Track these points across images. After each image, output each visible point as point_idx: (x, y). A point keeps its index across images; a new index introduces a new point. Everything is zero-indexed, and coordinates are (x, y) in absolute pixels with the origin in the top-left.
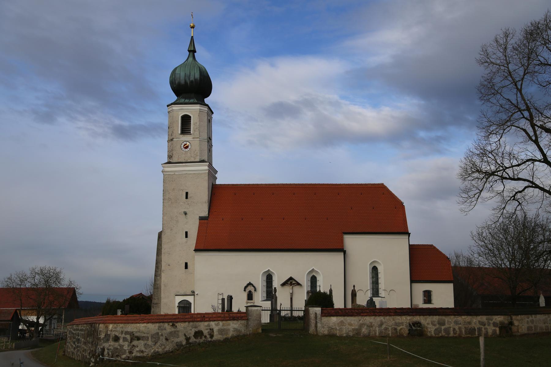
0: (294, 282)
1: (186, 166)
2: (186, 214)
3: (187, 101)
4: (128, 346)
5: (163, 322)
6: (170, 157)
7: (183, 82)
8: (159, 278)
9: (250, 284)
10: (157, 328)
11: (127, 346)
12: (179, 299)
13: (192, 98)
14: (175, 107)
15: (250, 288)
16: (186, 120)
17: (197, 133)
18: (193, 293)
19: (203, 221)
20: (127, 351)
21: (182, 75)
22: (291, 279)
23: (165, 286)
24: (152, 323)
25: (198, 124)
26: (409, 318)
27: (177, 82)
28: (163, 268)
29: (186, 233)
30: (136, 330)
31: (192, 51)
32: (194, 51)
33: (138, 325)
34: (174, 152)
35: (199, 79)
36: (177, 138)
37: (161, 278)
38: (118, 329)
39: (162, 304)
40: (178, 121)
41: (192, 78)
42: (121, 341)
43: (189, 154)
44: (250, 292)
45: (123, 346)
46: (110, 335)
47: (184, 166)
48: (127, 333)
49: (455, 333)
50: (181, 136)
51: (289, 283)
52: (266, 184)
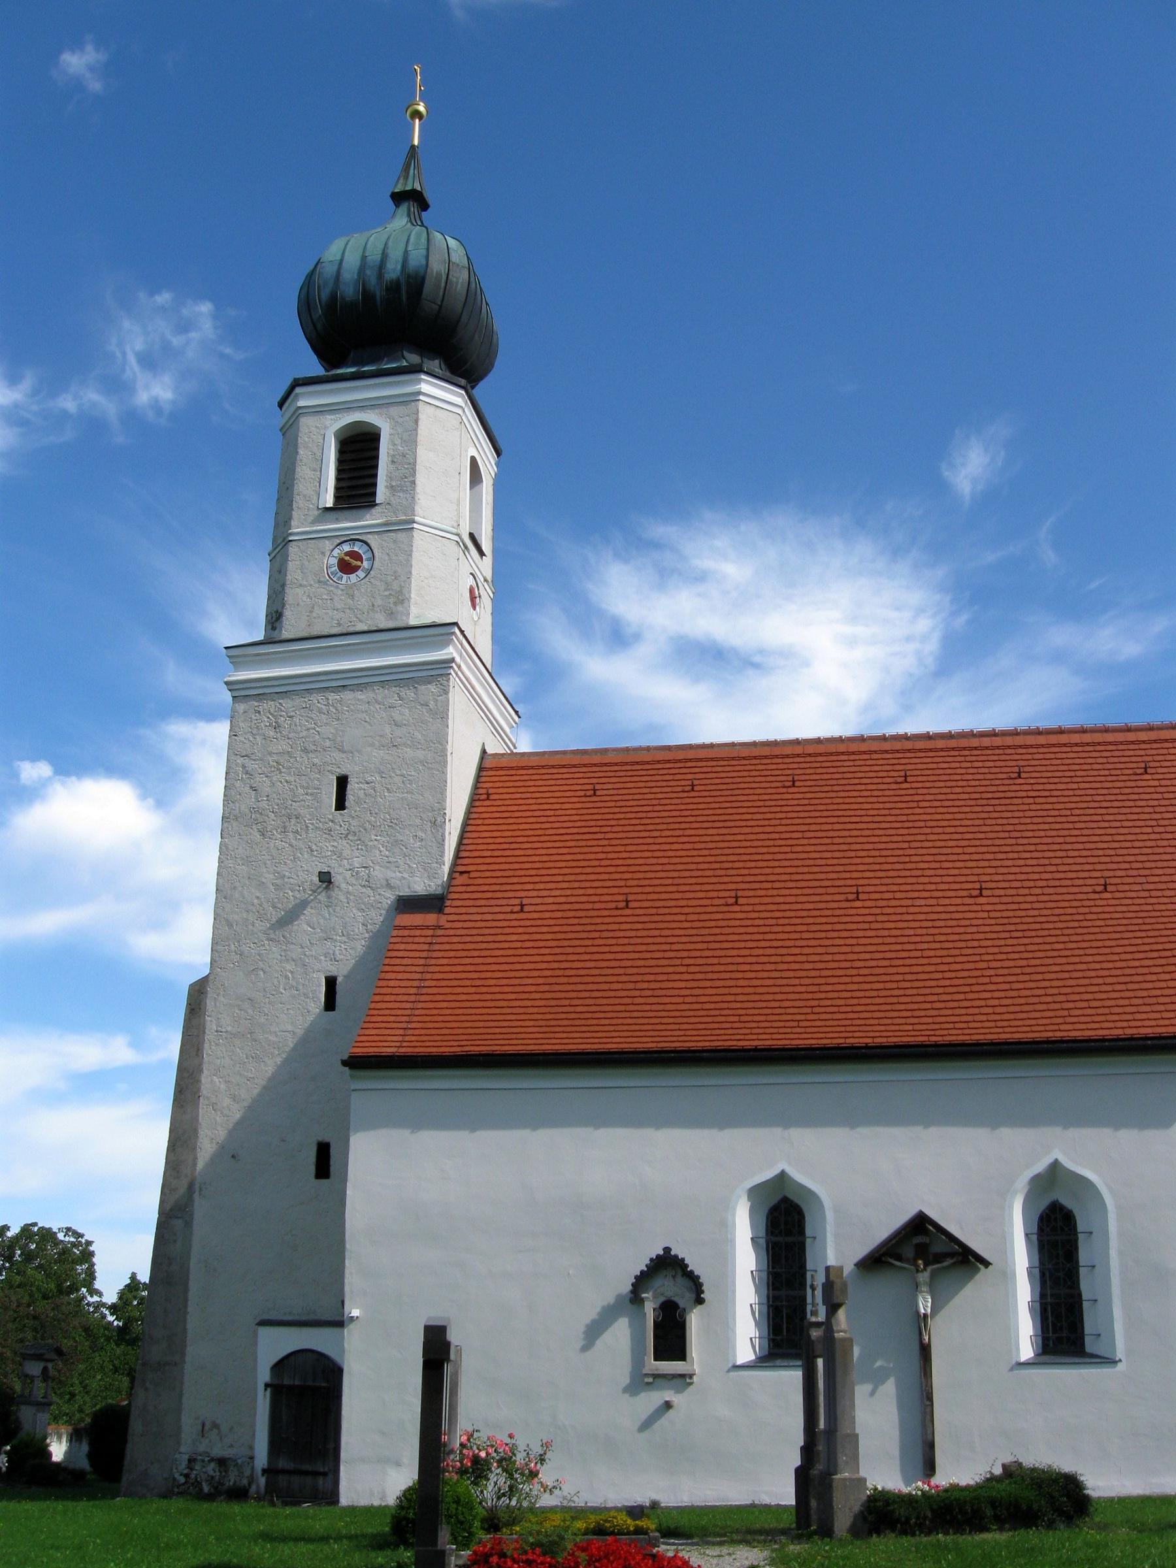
6: (275, 618)
7: (349, 291)
9: (667, 1264)
12: (276, 1344)
15: (668, 1287)
16: (359, 453)
22: (920, 1224)
37: (188, 1224)
39: (188, 1367)
43: (363, 601)
51: (909, 1252)
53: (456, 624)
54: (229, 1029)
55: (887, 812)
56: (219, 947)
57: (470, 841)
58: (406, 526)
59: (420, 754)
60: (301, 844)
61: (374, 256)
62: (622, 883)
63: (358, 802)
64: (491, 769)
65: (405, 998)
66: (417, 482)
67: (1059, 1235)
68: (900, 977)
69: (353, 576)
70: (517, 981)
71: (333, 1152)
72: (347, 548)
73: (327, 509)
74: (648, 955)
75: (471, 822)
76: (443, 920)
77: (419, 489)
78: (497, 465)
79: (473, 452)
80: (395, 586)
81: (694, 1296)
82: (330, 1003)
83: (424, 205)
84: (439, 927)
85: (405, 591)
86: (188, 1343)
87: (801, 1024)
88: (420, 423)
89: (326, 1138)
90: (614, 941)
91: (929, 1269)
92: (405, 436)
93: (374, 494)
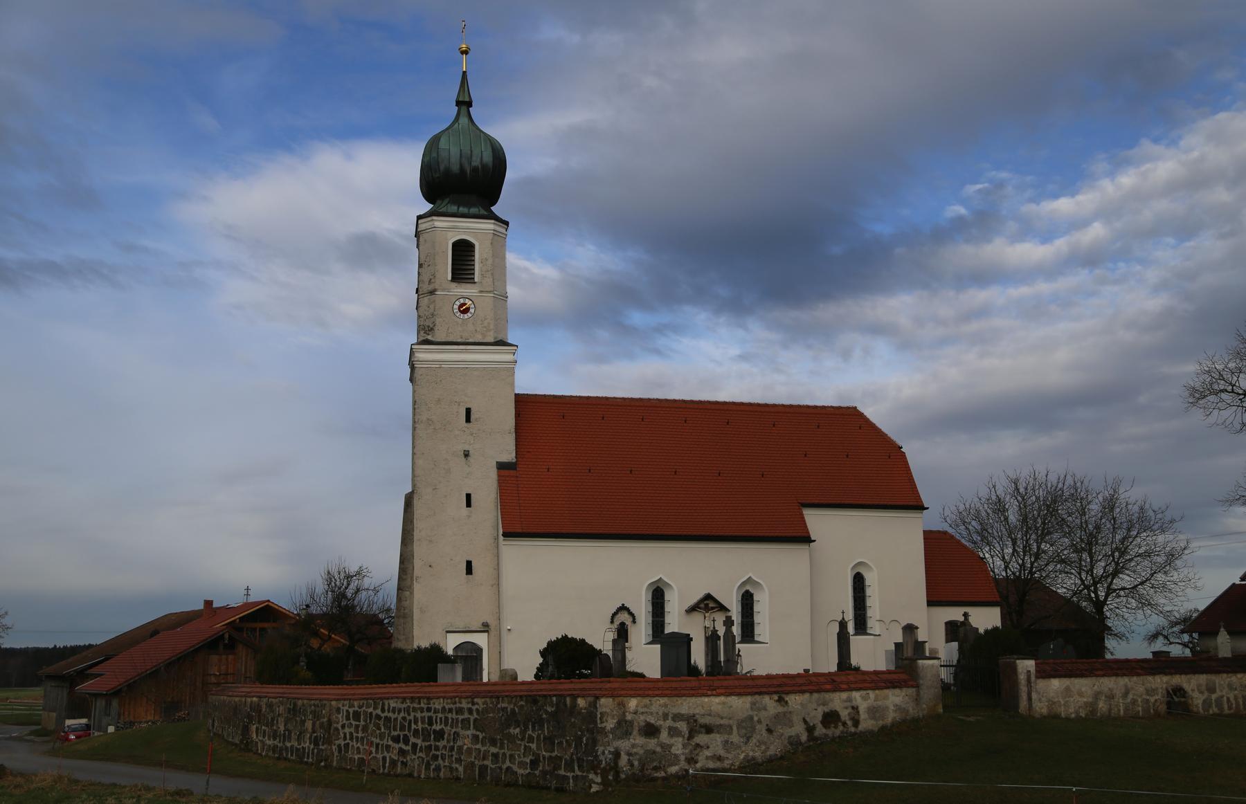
0: (711, 605)
1: (467, 351)
2: (466, 455)
3: (463, 210)
4: (684, 746)
5: (760, 693)
7: (455, 168)
8: (407, 593)
9: (623, 608)
10: (748, 705)
11: (680, 746)
13: (474, 205)
14: (440, 222)
15: (624, 617)
16: (463, 251)
17: (489, 280)
18: (485, 628)
19: (506, 472)
20: (682, 758)
21: (455, 152)
22: (708, 597)
23: (422, 611)
24: (739, 694)
25: (490, 262)
26: (1165, 679)
27: (442, 167)
28: (416, 572)
29: (468, 496)
30: (703, 712)
31: (464, 104)
32: (469, 104)
33: (706, 699)
34: (438, 321)
35: (491, 164)
36: (444, 290)
37: (412, 593)
38: (654, 709)
41: (476, 162)
42: (664, 735)
44: (623, 624)
45: (671, 746)
46: (631, 722)
47: (462, 351)
48: (677, 717)
49: (1230, 708)
50: (454, 285)
52: (624, 399)
67: (747, 601)
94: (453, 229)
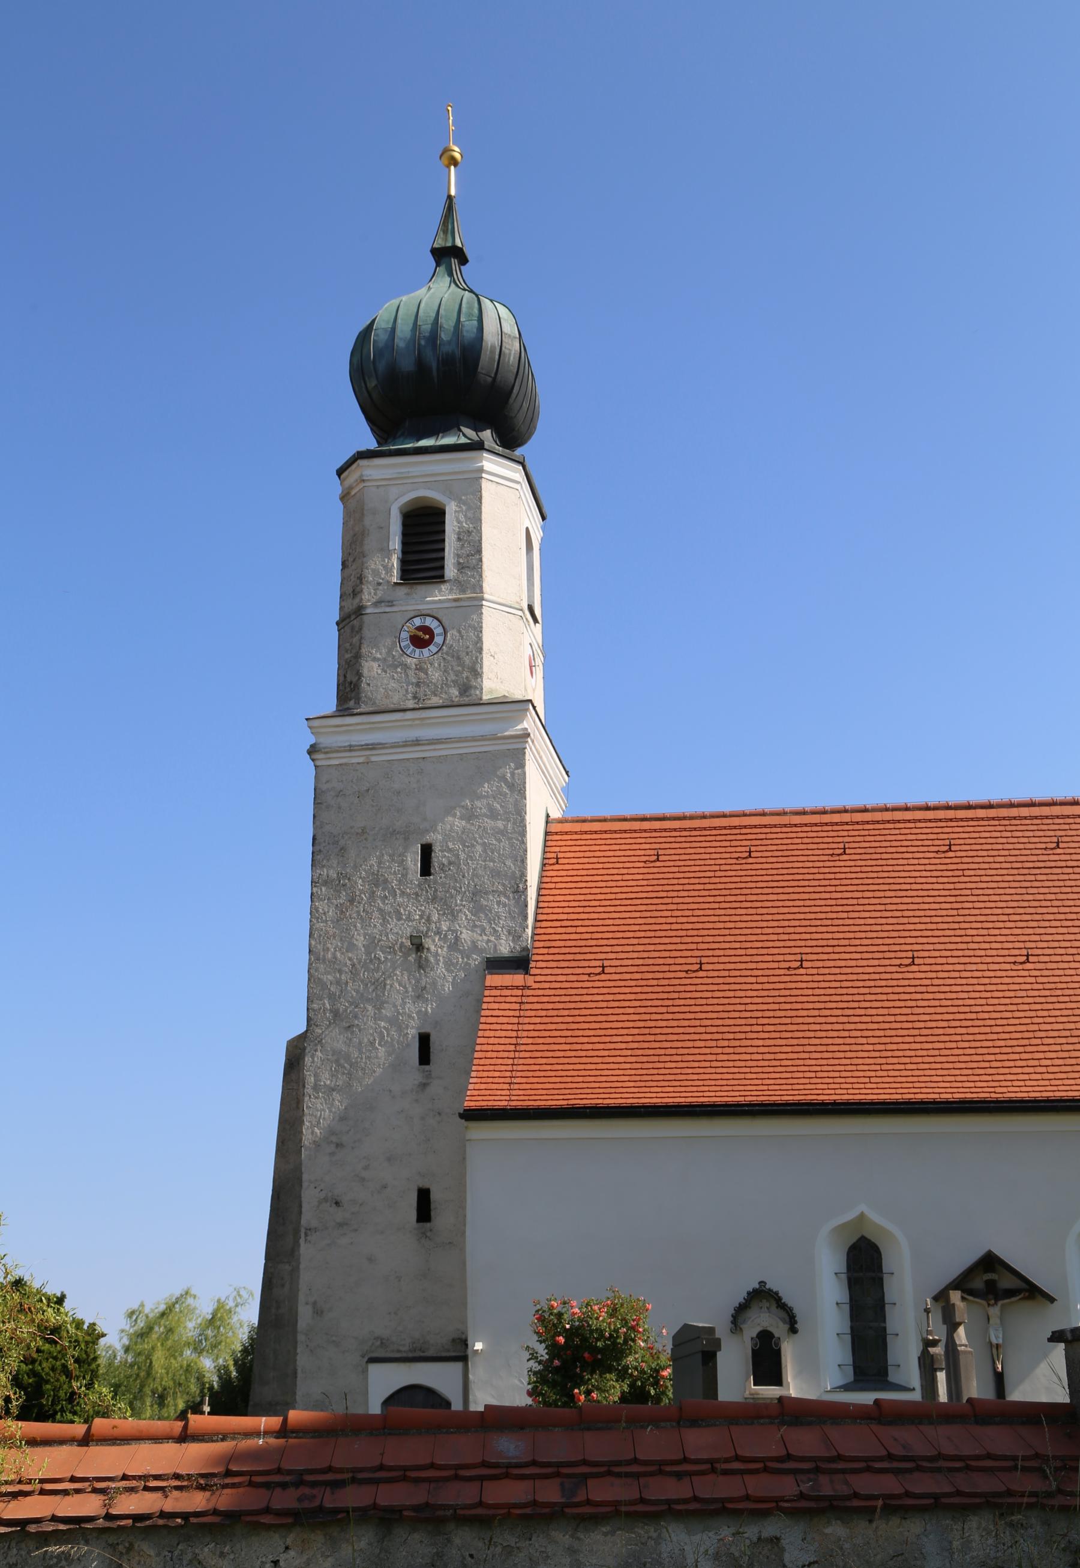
9: (761, 1295)
14: (376, 470)
16: (424, 527)
22: (990, 1262)
23: (318, 1312)
28: (308, 1217)
37: (295, 1270)
40: (384, 528)
50: (402, 591)
53: (530, 701)
54: (328, 1082)
55: (934, 880)
56: (315, 1006)
57: (546, 905)
58: (475, 604)
59: (500, 824)
60: (388, 908)
61: (426, 328)
62: (694, 946)
63: (442, 867)
64: (556, 833)
65: (506, 1054)
66: (484, 559)
68: (959, 1038)
69: (425, 651)
70: (608, 1039)
71: (434, 1196)
72: (418, 622)
73: (396, 584)
74: (726, 1015)
75: (544, 886)
76: (530, 981)
77: (485, 567)
78: (543, 528)
79: (527, 524)
80: (467, 660)
81: (787, 1327)
82: (425, 1057)
83: (463, 260)
84: (529, 988)
85: (478, 667)
86: (298, 1383)
87: (872, 1080)
88: (483, 501)
89: (425, 1184)
90: (692, 1002)
91: (1000, 1303)
92: (470, 514)
93: (442, 567)
94: (407, 478)
